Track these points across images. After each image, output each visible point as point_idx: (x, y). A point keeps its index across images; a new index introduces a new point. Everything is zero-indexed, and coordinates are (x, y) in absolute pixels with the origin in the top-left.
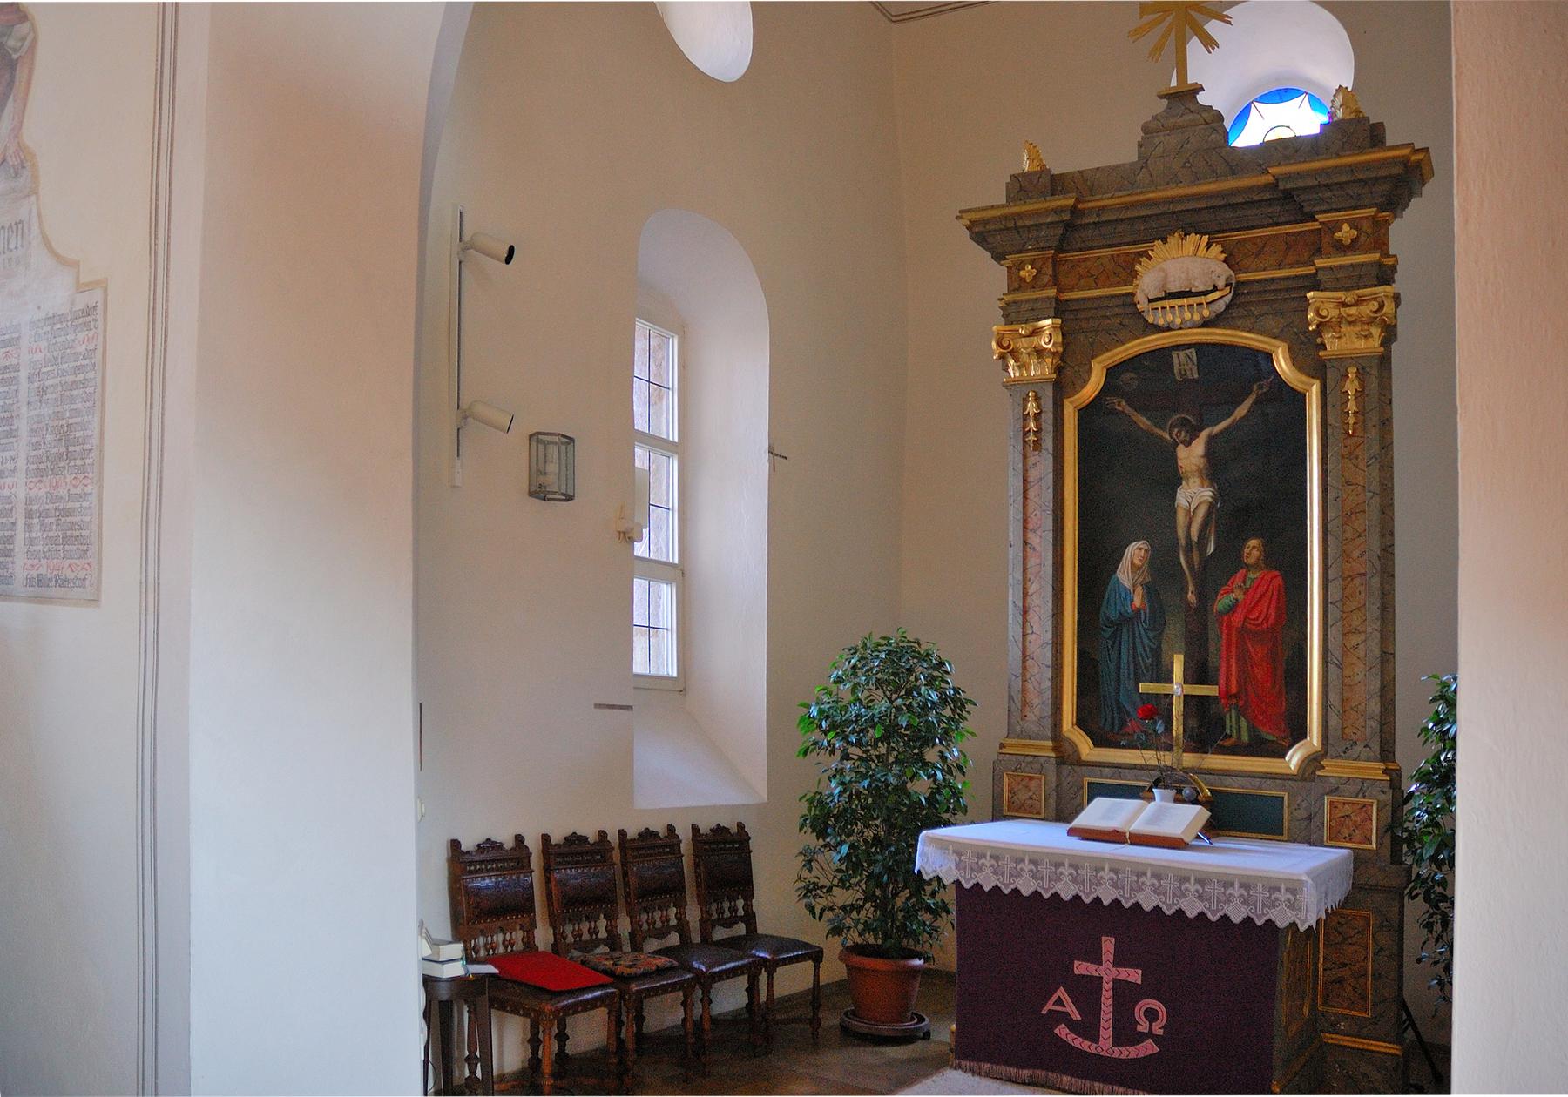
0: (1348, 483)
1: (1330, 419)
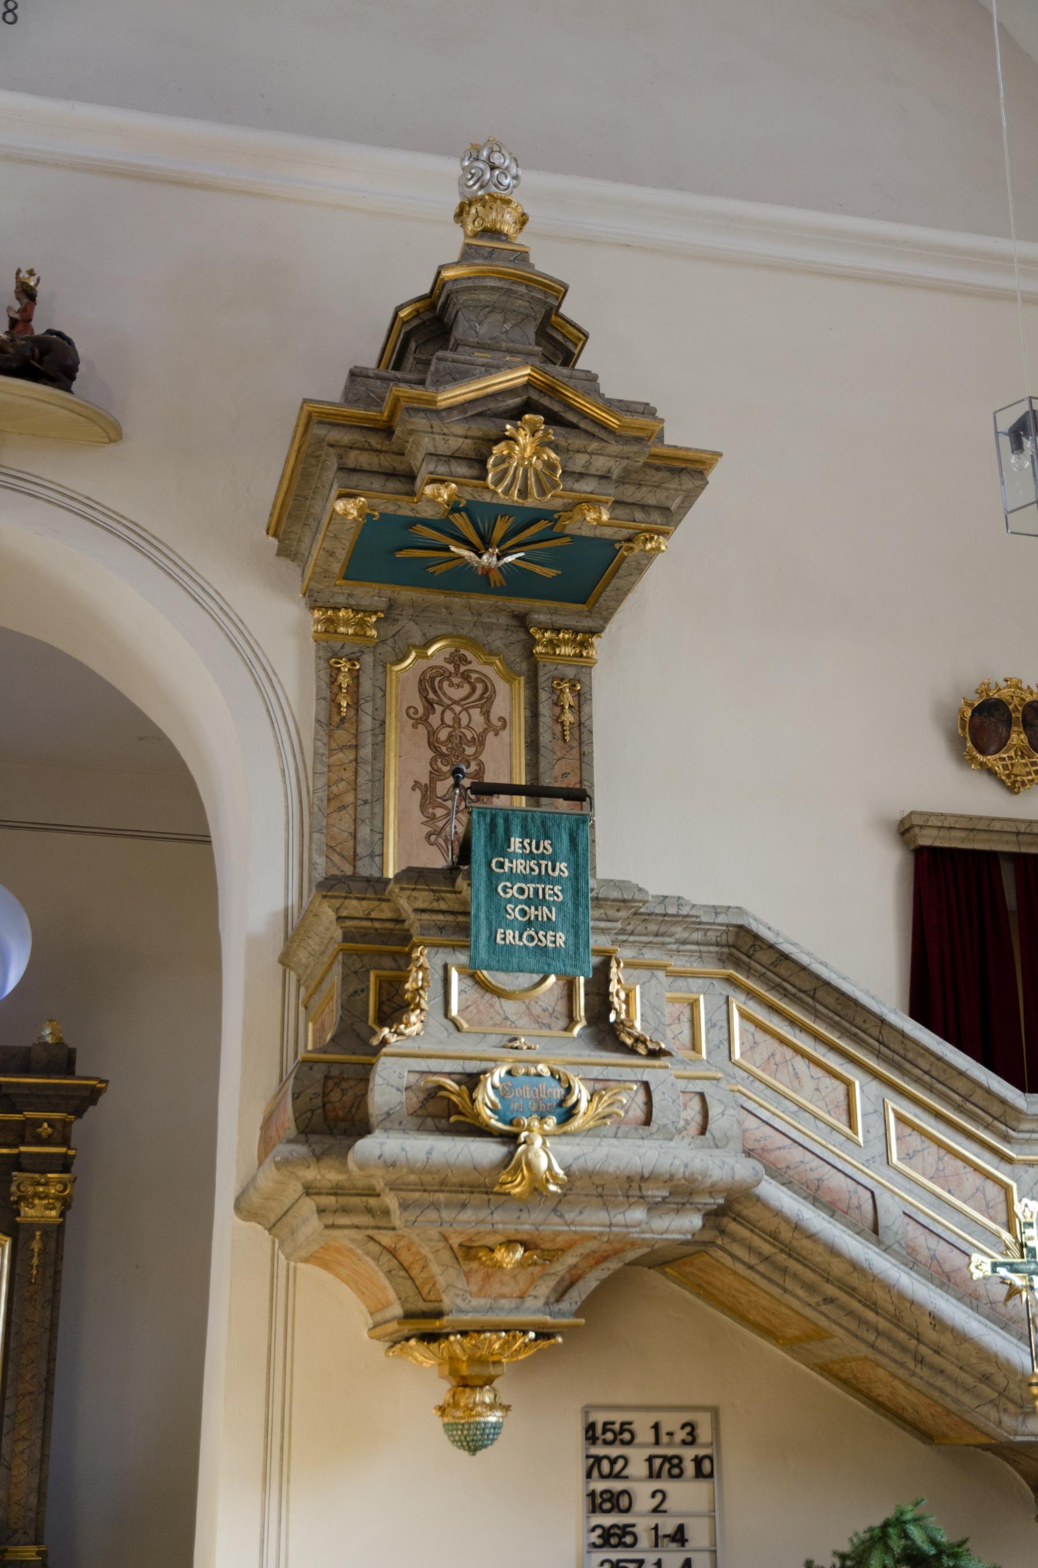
0: (27, 1321)
1: (18, 1271)
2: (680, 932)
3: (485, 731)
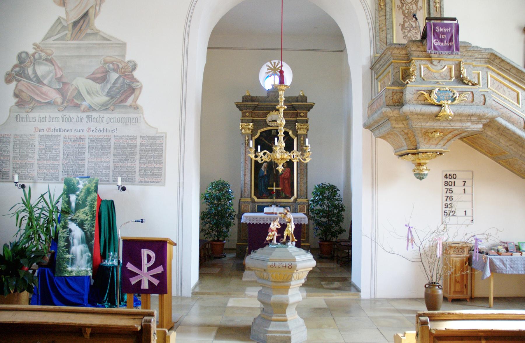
2: (476, 55)
3: (417, 10)
